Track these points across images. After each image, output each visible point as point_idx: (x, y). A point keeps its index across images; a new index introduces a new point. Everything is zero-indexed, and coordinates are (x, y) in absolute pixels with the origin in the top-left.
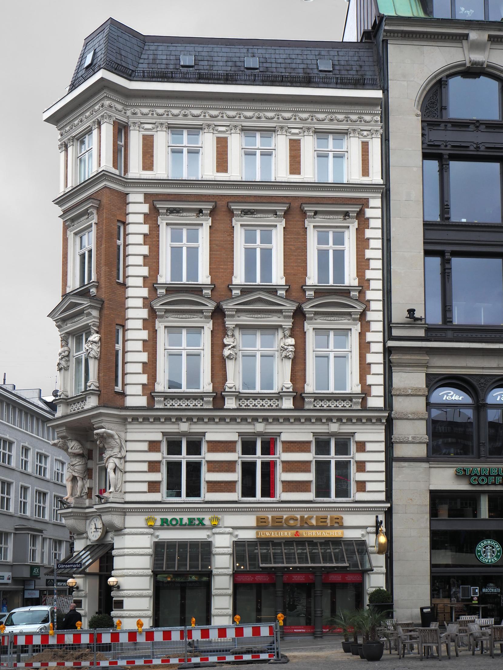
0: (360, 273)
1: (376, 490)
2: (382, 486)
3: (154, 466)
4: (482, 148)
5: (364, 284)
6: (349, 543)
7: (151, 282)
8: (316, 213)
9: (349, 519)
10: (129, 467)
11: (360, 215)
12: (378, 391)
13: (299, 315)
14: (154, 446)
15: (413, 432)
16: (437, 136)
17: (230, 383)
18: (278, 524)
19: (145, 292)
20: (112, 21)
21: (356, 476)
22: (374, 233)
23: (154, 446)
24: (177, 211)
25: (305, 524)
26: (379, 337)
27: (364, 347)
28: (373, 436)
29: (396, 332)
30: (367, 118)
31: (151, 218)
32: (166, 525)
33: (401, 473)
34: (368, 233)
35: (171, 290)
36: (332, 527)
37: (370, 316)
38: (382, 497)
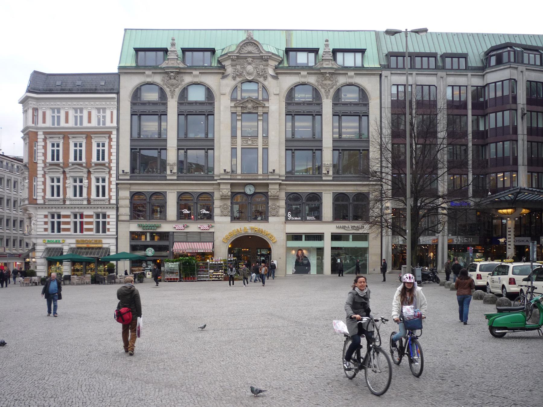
2: (115, 230)
3: (46, 223)
5: (110, 161)
6: (104, 248)
7: (44, 162)
9: (104, 241)
10: (38, 223)
12: (114, 198)
13: (89, 173)
14: (46, 216)
15: (125, 211)
16: (291, 108)
17: (67, 196)
19: (43, 165)
21: (107, 226)
22: (114, 144)
23: (46, 216)
24: (52, 137)
25: (90, 242)
26: (115, 179)
27: (110, 183)
28: (112, 213)
29: (120, 178)
30: (112, 103)
31: (45, 140)
32: (49, 242)
33: (121, 226)
34: (112, 143)
35: (51, 165)
36: (99, 244)
37: (112, 172)
38: (115, 233)
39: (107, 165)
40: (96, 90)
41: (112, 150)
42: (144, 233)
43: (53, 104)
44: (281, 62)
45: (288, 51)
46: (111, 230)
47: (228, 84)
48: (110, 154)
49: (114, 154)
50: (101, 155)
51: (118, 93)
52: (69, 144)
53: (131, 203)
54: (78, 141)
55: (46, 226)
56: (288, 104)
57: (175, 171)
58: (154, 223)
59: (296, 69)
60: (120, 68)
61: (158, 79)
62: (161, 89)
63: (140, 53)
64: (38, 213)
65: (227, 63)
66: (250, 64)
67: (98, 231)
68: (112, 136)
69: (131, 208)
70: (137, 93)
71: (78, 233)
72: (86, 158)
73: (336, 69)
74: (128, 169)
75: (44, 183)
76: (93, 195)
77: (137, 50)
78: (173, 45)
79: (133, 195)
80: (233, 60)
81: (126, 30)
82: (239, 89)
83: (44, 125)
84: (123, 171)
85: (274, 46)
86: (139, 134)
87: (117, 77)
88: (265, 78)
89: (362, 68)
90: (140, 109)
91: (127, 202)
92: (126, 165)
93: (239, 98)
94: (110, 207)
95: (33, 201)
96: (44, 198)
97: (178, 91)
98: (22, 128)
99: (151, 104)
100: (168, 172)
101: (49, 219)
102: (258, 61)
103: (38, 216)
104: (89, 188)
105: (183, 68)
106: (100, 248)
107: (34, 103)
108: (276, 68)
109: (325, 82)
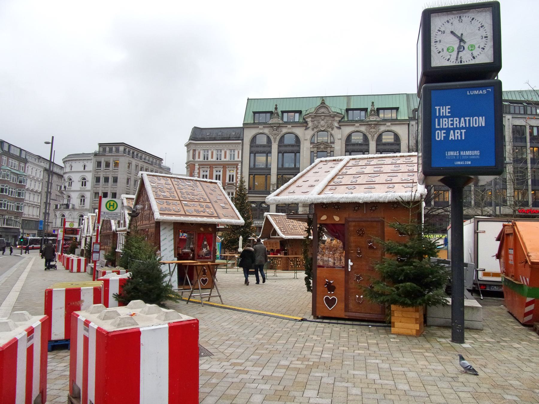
0: (236, 180)
22: (239, 171)
31: (199, 169)
34: (238, 171)
40: (230, 138)
41: (238, 176)
43: (205, 147)
44: (343, 118)
45: (347, 110)
47: (309, 133)
48: (237, 178)
51: (242, 140)
56: (346, 145)
59: (352, 122)
60: (244, 124)
61: (266, 131)
63: (257, 115)
65: (309, 120)
66: (323, 120)
70: (254, 139)
73: (378, 121)
77: (255, 113)
78: (276, 109)
80: (312, 118)
81: (248, 99)
82: (316, 136)
83: (199, 160)
85: (339, 107)
86: (254, 165)
87: (242, 129)
88: (333, 129)
89: (396, 120)
90: (256, 149)
93: (316, 142)
97: (278, 138)
98: (186, 162)
102: (328, 118)
105: (282, 124)
108: (340, 121)
109: (371, 130)
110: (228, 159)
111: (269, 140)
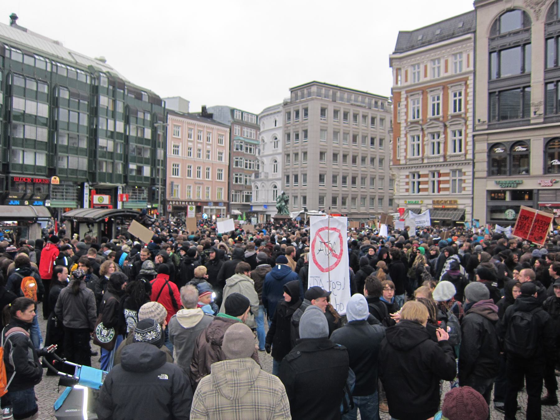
1: (468, 190)
2: (471, 189)
3: (407, 183)
4: (511, 44)
8: (452, 87)
9: (460, 201)
10: (401, 184)
11: (466, 84)
12: (470, 152)
13: (445, 126)
15: (483, 166)
17: (425, 154)
18: (438, 202)
20: (400, 33)
22: (470, 90)
23: (407, 177)
26: (471, 130)
28: (468, 170)
29: (477, 128)
31: (406, 99)
34: (468, 90)
37: (468, 123)
38: (471, 193)
39: (463, 116)
40: (453, 34)
42: (504, 192)
43: (413, 61)
46: (466, 189)
48: (466, 103)
49: (471, 102)
50: (458, 105)
51: (475, 32)
52: (427, 99)
53: (489, 156)
54: (435, 93)
55: (407, 187)
57: (541, 111)
58: (514, 180)
62: (524, 13)
64: (401, 174)
67: (454, 191)
68: (468, 82)
69: (488, 162)
71: (436, 193)
72: (443, 111)
74: (485, 118)
75: (406, 143)
76: (450, 152)
79: (492, 147)
84: (479, 120)
86: (499, 74)
91: (485, 156)
92: (483, 113)
94: (466, 163)
95: (396, 162)
96: (405, 157)
99: (512, 35)
100: (532, 115)
101: (411, 179)
103: (401, 177)
104: (445, 143)
106: (455, 209)
107: (398, 63)
110: (450, 72)
111: (526, 19)
